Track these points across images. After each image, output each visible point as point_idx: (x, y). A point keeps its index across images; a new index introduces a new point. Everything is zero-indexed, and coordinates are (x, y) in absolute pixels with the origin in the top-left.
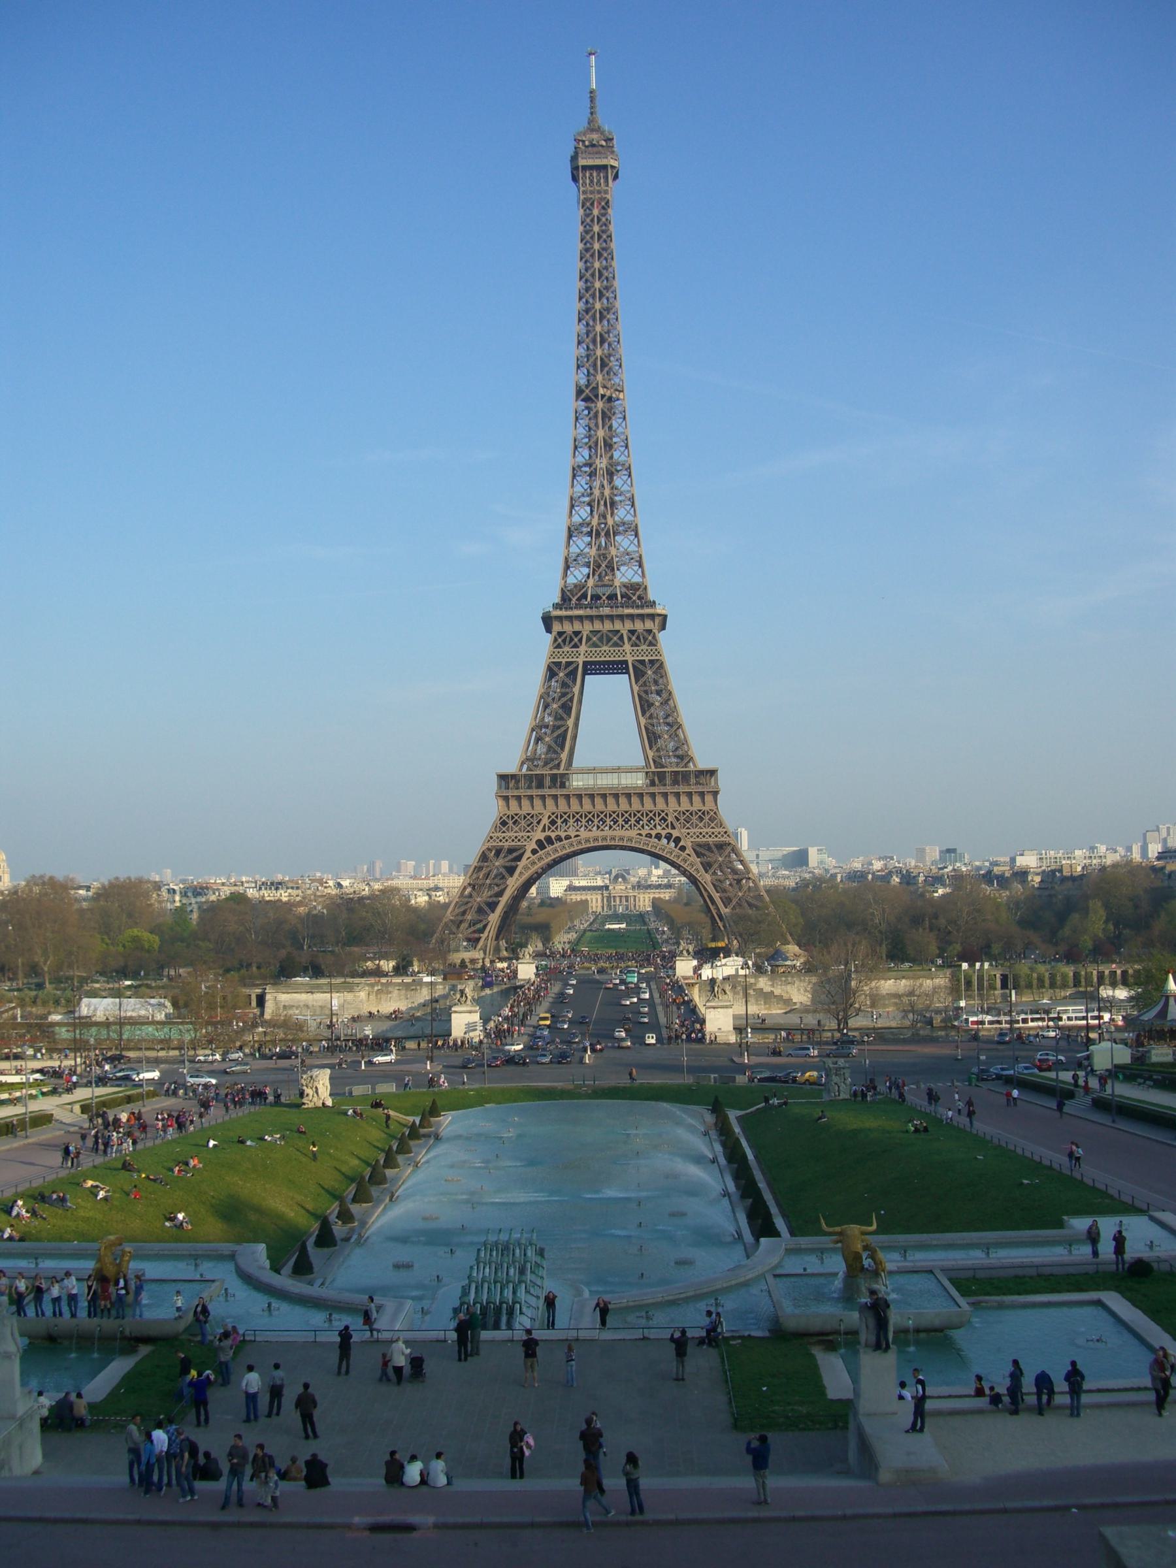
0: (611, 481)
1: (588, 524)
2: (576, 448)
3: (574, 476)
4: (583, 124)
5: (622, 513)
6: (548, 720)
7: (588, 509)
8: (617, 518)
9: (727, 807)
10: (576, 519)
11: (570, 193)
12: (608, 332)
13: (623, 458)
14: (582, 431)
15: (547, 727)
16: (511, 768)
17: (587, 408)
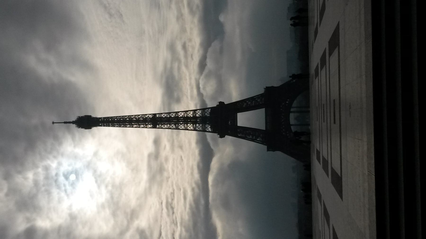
0: (181, 117)
1: (193, 125)
2: (170, 128)
3: (179, 129)
4: (74, 126)
5: (191, 114)
6: (251, 137)
7: (189, 125)
8: (192, 116)
9: (276, 84)
10: (192, 128)
11: (95, 129)
12: (136, 118)
13: (174, 115)
14: (166, 126)
15: (253, 137)
16: (266, 147)
17: (159, 125)
